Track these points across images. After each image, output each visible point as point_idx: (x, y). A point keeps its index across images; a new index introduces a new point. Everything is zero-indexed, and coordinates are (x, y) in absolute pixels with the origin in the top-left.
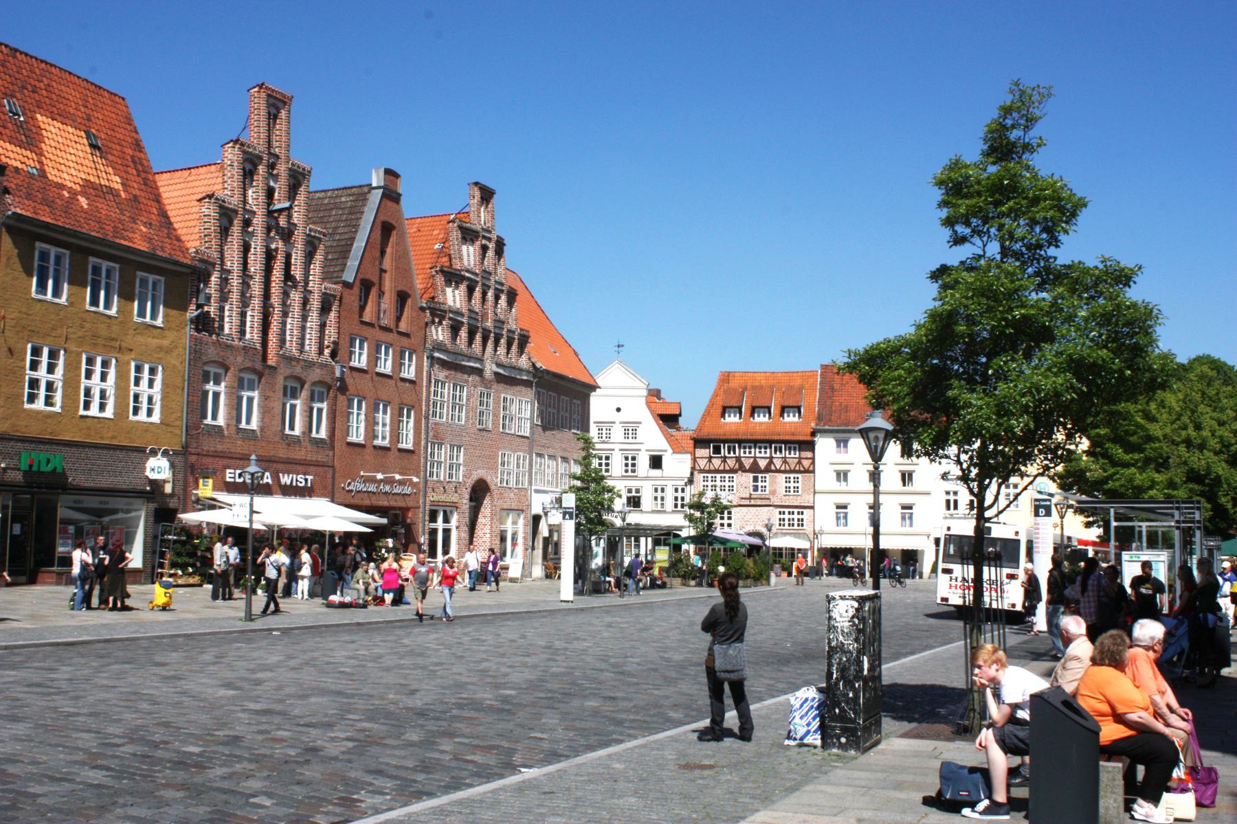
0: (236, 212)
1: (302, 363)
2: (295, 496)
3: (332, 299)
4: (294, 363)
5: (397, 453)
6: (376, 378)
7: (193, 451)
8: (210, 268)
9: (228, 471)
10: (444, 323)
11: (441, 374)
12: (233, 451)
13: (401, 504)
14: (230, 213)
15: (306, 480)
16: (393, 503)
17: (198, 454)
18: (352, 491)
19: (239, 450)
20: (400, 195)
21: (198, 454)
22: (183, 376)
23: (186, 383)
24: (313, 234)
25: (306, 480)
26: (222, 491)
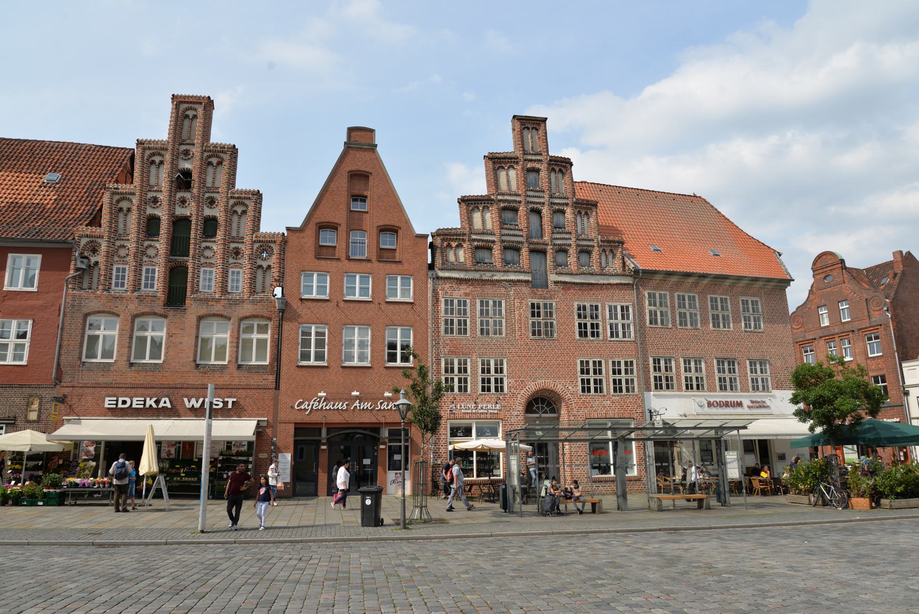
0: (134, 194)
1: (222, 302)
4: (210, 303)
5: (385, 372)
6: (342, 304)
7: (65, 385)
8: (99, 240)
9: (107, 399)
10: (465, 245)
11: (459, 293)
14: (128, 196)
15: (226, 403)
17: (73, 387)
18: (305, 410)
19: (129, 381)
21: (73, 387)
23: (59, 330)
24: (236, 195)
25: (226, 403)
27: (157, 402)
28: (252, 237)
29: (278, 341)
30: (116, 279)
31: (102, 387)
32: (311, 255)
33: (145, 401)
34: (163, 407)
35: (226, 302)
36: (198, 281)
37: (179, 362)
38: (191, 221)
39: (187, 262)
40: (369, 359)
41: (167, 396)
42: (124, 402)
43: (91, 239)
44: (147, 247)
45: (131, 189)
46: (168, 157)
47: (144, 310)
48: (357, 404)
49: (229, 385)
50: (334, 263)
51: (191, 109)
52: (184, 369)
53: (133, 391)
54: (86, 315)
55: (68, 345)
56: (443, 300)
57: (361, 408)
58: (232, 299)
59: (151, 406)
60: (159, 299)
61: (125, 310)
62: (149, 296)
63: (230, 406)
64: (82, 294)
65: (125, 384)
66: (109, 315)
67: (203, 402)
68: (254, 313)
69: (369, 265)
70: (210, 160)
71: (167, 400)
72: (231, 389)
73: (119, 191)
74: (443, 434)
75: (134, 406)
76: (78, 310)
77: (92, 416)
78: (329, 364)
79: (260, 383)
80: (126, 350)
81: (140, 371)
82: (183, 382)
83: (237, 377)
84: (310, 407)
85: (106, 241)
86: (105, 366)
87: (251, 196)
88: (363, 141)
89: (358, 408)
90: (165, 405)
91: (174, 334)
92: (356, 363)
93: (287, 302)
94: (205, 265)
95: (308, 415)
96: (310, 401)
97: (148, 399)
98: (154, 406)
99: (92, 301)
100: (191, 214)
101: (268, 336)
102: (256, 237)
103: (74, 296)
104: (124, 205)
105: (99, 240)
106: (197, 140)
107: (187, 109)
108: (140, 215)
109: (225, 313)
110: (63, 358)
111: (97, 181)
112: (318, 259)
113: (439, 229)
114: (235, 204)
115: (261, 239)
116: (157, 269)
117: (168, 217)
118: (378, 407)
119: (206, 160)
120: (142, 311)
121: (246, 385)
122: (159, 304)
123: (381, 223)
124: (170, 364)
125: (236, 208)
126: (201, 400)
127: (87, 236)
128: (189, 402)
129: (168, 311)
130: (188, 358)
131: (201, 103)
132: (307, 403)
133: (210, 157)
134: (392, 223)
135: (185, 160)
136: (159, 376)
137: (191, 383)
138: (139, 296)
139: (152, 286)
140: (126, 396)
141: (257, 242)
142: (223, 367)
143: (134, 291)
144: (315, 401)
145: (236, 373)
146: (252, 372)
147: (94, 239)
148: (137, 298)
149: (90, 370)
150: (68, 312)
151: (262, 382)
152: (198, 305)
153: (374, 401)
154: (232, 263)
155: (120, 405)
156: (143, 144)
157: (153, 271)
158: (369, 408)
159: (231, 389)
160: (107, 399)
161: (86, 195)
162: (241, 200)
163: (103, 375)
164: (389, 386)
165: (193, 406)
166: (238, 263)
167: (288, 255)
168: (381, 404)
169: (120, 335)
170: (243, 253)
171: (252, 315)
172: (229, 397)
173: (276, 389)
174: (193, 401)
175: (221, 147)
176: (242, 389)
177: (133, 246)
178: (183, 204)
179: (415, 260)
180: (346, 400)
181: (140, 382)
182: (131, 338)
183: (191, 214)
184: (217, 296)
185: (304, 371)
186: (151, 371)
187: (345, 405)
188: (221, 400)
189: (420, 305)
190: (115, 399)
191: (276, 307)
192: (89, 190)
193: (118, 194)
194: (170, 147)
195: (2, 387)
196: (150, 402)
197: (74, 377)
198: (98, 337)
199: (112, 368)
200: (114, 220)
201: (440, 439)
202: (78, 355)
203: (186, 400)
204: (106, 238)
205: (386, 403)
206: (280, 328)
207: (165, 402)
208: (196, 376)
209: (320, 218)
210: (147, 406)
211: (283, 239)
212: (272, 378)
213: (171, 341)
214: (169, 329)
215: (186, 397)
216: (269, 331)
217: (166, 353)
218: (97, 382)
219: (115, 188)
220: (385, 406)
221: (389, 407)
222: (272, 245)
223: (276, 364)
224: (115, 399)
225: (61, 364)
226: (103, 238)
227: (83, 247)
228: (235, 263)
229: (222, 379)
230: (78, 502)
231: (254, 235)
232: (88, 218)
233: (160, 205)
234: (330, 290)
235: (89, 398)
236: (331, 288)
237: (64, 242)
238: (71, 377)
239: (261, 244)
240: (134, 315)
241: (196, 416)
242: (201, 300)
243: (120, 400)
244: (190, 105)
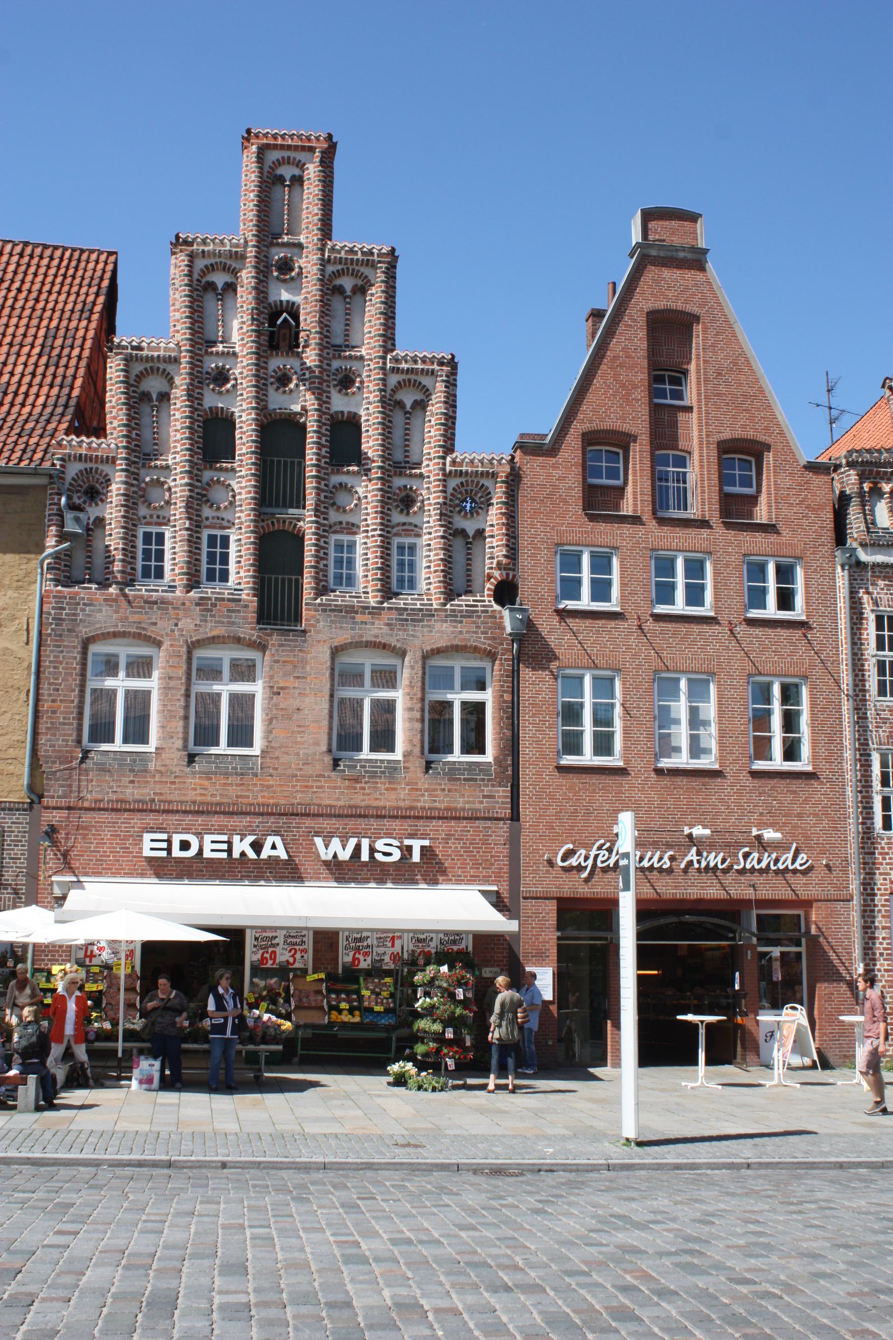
0: (176, 361)
1: (385, 616)
2: (267, 880)
3: (488, 483)
4: (359, 618)
5: (749, 782)
6: (650, 625)
7: (52, 802)
8: (106, 468)
9: (147, 837)
12: (175, 797)
13: (779, 891)
16: (740, 890)
17: (69, 808)
18: (580, 868)
19: (191, 795)
20: (705, 252)
21: (69, 808)
22: (29, 666)
24: (404, 366)
26: (142, 875)
27: (257, 846)
28: (444, 464)
29: (513, 708)
30: (143, 560)
31: (133, 810)
32: (576, 507)
33: (230, 843)
34: (270, 857)
35: (394, 615)
36: (326, 565)
37: (298, 754)
38: (303, 427)
39: (299, 520)
40: (714, 752)
41: (276, 833)
42: (185, 845)
43: (89, 465)
44: (208, 484)
45: (170, 350)
46: (247, 276)
47: (215, 633)
48: (692, 855)
49: (411, 808)
50: (627, 529)
51: (288, 161)
52: (308, 770)
53: (200, 819)
54: (86, 644)
55: (54, 712)
56: (872, 617)
57: (703, 864)
58: (406, 609)
59: (243, 854)
60: (246, 606)
61: (172, 631)
62: (223, 599)
63: (416, 857)
64: (77, 593)
65: (182, 802)
66: (136, 641)
67: (358, 848)
68: (456, 642)
69: (705, 533)
70: (338, 282)
71: (278, 840)
72: (415, 817)
73: (145, 353)
74: (884, 928)
75: (207, 854)
76: (69, 630)
77: (114, 874)
78: (626, 761)
79: (477, 806)
80: (181, 723)
81: (212, 773)
82: (308, 800)
83: (426, 790)
84: (590, 862)
85: (122, 470)
86: (134, 761)
87: (436, 367)
88: (676, 241)
89: (696, 865)
90: (274, 853)
91: (282, 688)
92: (682, 760)
93: (530, 620)
94: (338, 528)
95: (587, 880)
96: (588, 847)
97: (236, 839)
98: (251, 854)
99: (100, 611)
100: (304, 408)
101: (488, 697)
102: (454, 462)
103: (59, 597)
104: (154, 385)
105: (106, 468)
106: (308, 236)
107: (279, 163)
108: (193, 409)
109: (393, 642)
110: (42, 740)
111: (57, 328)
112: (592, 518)
113: (522, 435)
114: (400, 385)
115: (464, 469)
116: (232, 538)
117: (257, 414)
118: (738, 863)
119: (330, 280)
120: (209, 635)
121: (447, 809)
122: (244, 618)
123: (726, 435)
124: (277, 758)
125: (399, 396)
126: (352, 842)
127: (80, 459)
128: (327, 846)
129: (267, 635)
130: (317, 744)
131: (312, 150)
132: (583, 852)
133: (338, 274)
134: (750, 434)
135: (285, 281)
136: (255, 785)
137: (328, 802)
138: (201, 598)
139: (224, 576)
140: (186, 831)
141: (455, 476)
142: (393, 767)
143: (190, 587)
144: (599, 848)
145: (424, 781)
146: (459, 779)
147: (94, 466)
148: (198, 604)
149: (103, 769)
150: (50, 635)
151: (482, 802)
152: (332, 622)
153: (731, 847)
154: (398, 525)
155: (176, 853)
156: (191, 244)
157: (225, 541)
158: (720, 866)
159: (415, 817)
160: (147, 837)
161: (44, 360)
162: (413, 377)
163: (132, 782)
164: (761, 814)
165: (335, 856)
166: (410, 524)
167: (525, 507)
168: (746, 856)
169: (166, 690)
170: (423, 501)
171: (452, 646)
172: (412, 836)
173: (512, 819)
174: (336, 843)
175: (363, 253)
176: (440, 818)
177: (178, 482)
178: (286, 385)
179: (805, 522)
180: (669, 846)
181: (214, 800)
182: (82, 691)
183: (304, 408)
184: (373, 601)
185: (574, 779)
186: (236, 774)
187: (666, 858)
188: (396, 843)
189: (822, 626)
190: (164, 836)
191: (504, 628)
192: (47, 349)
193: (141, 359)
194: (251, 252)
195: (3, 809)
196: (242, 846)
197: (70, 786)
198: (114, 692)
199: (152, 766)
200: (133, 424)
201: (874, 938)
202: (75, 734)
203: (319, 841)
204: (121, 464)
205: (756, 855)
206: (514, 675)
207: (274, 847)
208: (335, 788)
209: (591, 422)
210: (236, 854)
211: (512, 468)
212: (502, 793)
213: (276, 705)
214: (271, 677)
215: (317, 834)
216: (156, 674)
217: (268, 732)
218: (121, 796)
219: (133, 348)
220: (755, 862)
221: (763, 865)
222: (488, 483)
223: (509, 762)
224: (164, 836)
225: (41, 753)
226: (114, 462)
227: (71, 484)
228: (404, 524)
229: (392, 795)
230: (470, 1081)
231: (449, 459)
232: (63, 415)
233: (234, 386)
234: (622, 591)
235: (107, 834)
236: (623, 585)
237: (35, 473)
238: (62, 786)
239: (463, 480)
240: (336, 647)
241: (338, 880)
242: (338, 609)
243: (177, 839)
244: (286, 154)
